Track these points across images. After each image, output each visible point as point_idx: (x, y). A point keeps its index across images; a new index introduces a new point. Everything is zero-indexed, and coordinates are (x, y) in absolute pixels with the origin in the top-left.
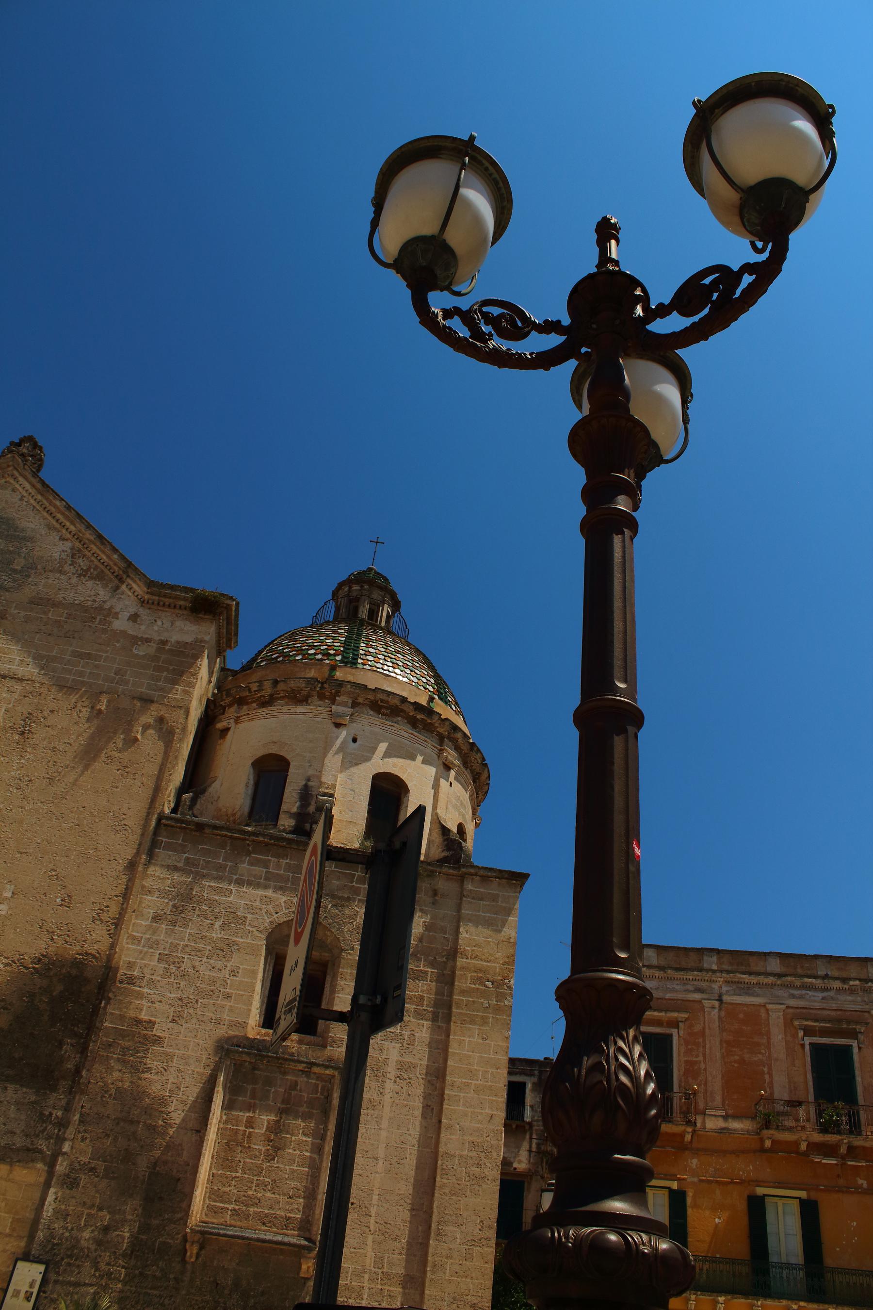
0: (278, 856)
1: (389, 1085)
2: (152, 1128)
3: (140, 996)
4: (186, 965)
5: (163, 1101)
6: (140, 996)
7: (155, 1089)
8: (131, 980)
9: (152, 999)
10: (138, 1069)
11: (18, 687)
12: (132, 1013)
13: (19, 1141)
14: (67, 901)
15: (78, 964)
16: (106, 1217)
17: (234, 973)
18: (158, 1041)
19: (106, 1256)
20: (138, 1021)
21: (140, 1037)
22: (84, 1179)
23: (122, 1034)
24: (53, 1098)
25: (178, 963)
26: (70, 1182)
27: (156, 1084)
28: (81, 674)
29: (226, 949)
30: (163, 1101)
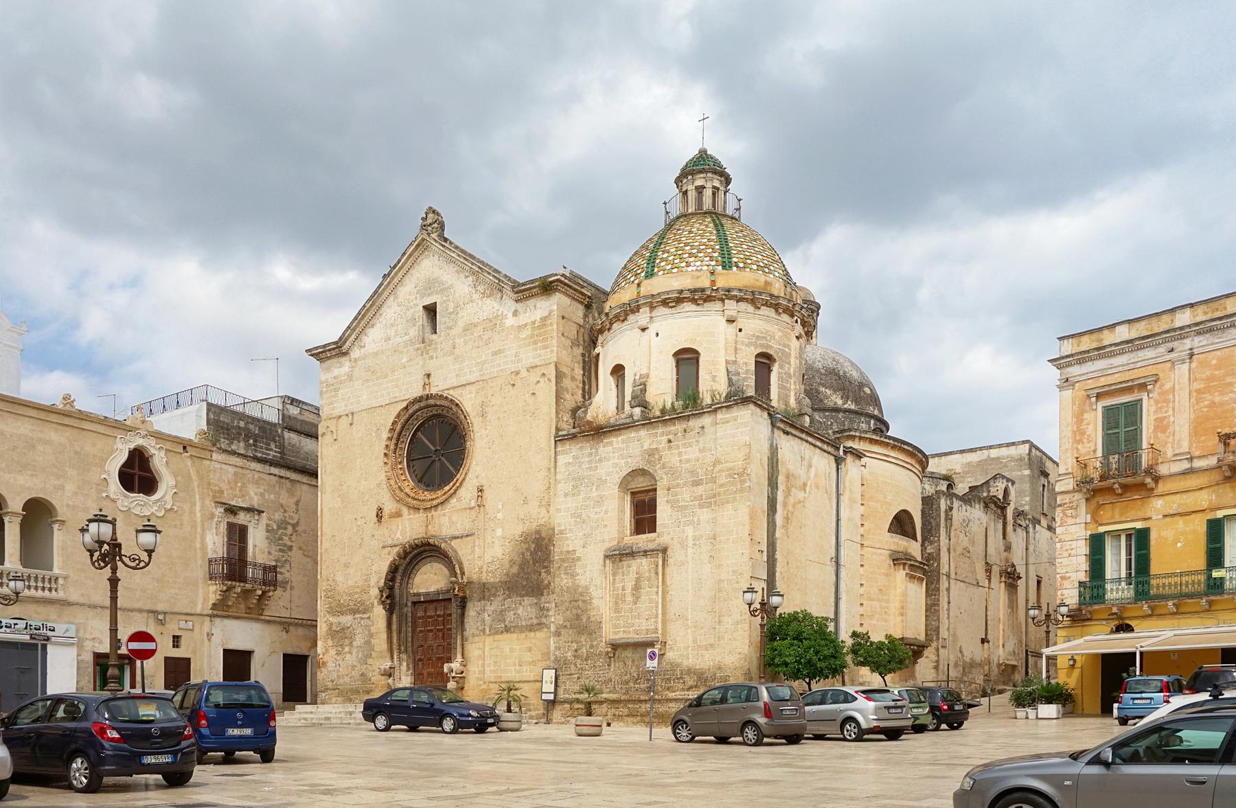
0: (617, 436)
1: (690, 550)
2: (584, 601)
3: (567, 539)
4: (584, 516)
5: (587, 588)
6: (567, 539)
7: (583, 583)
8: (561, 532)
9: (571, 540)
10: (573, 576)
11: (473, 388)
12: (565, 549)
13: (535, 621)
14: (525, 501)
15: (538, 532)
16: (575, 645)
17: (606, 512)
18: (579, 559)
19: (579, 661)
20: (568, 552)
21: (572, 559)
22: (563, 632)
23: (563, 560)
24: (543, 599)
25: (580, 516)
26: (558, 634)
27: (582, 580)
28: (499, 365)
29: (599, 501)
30: (587, 588)
